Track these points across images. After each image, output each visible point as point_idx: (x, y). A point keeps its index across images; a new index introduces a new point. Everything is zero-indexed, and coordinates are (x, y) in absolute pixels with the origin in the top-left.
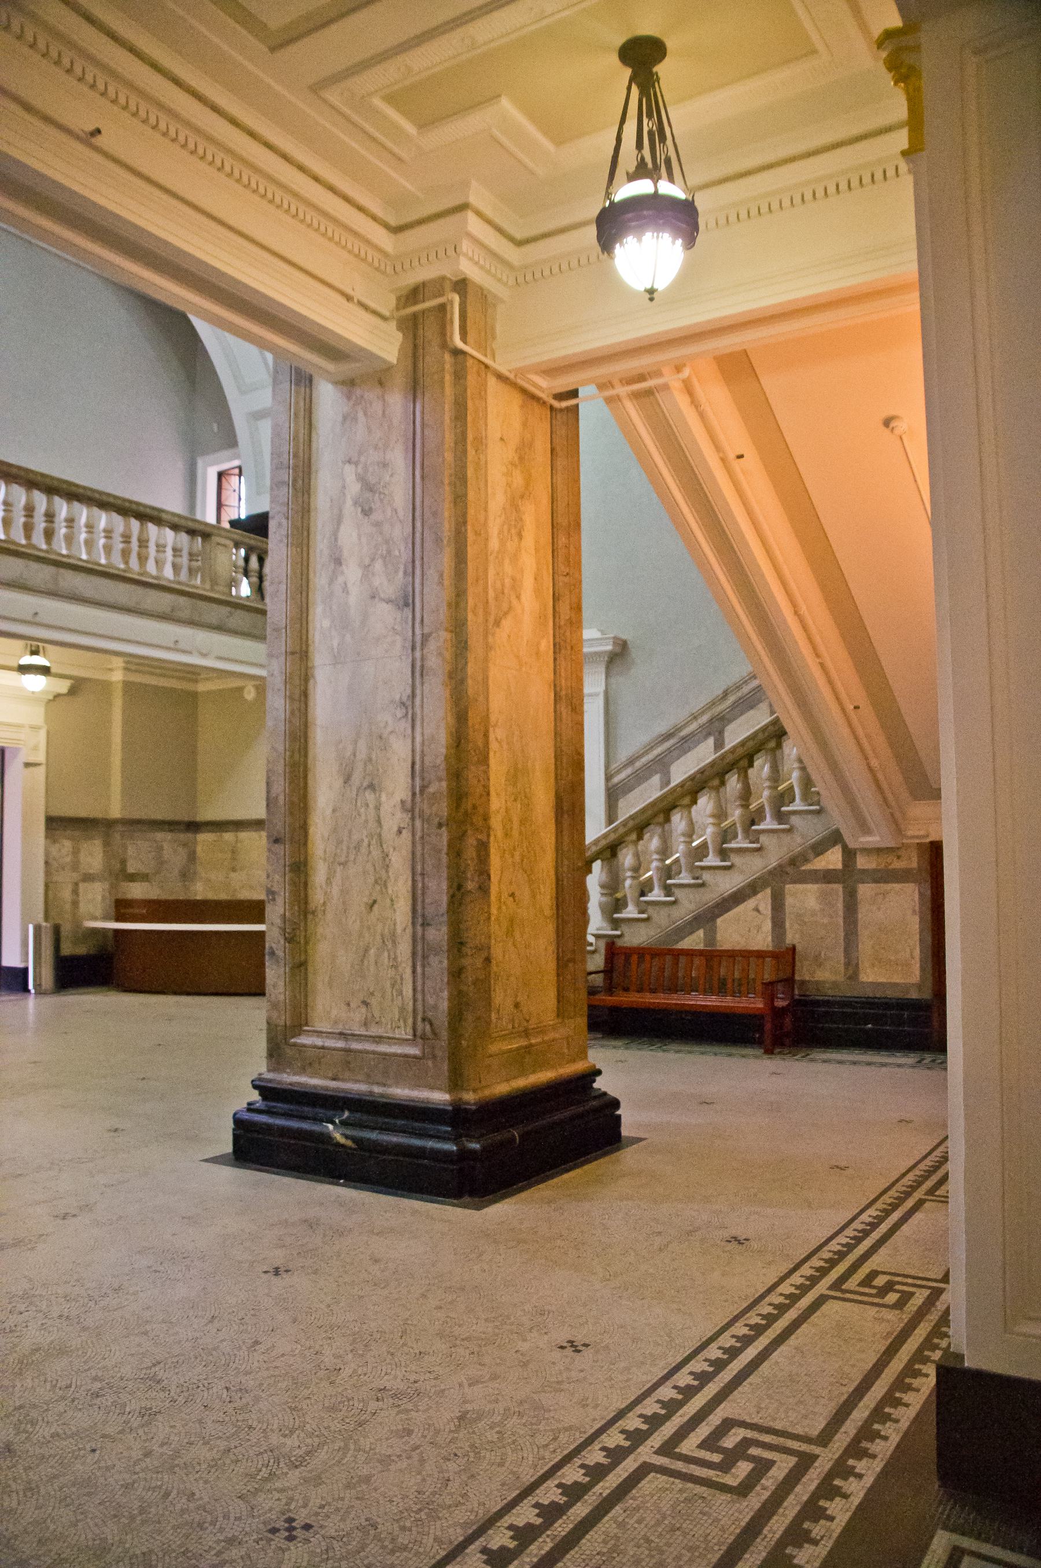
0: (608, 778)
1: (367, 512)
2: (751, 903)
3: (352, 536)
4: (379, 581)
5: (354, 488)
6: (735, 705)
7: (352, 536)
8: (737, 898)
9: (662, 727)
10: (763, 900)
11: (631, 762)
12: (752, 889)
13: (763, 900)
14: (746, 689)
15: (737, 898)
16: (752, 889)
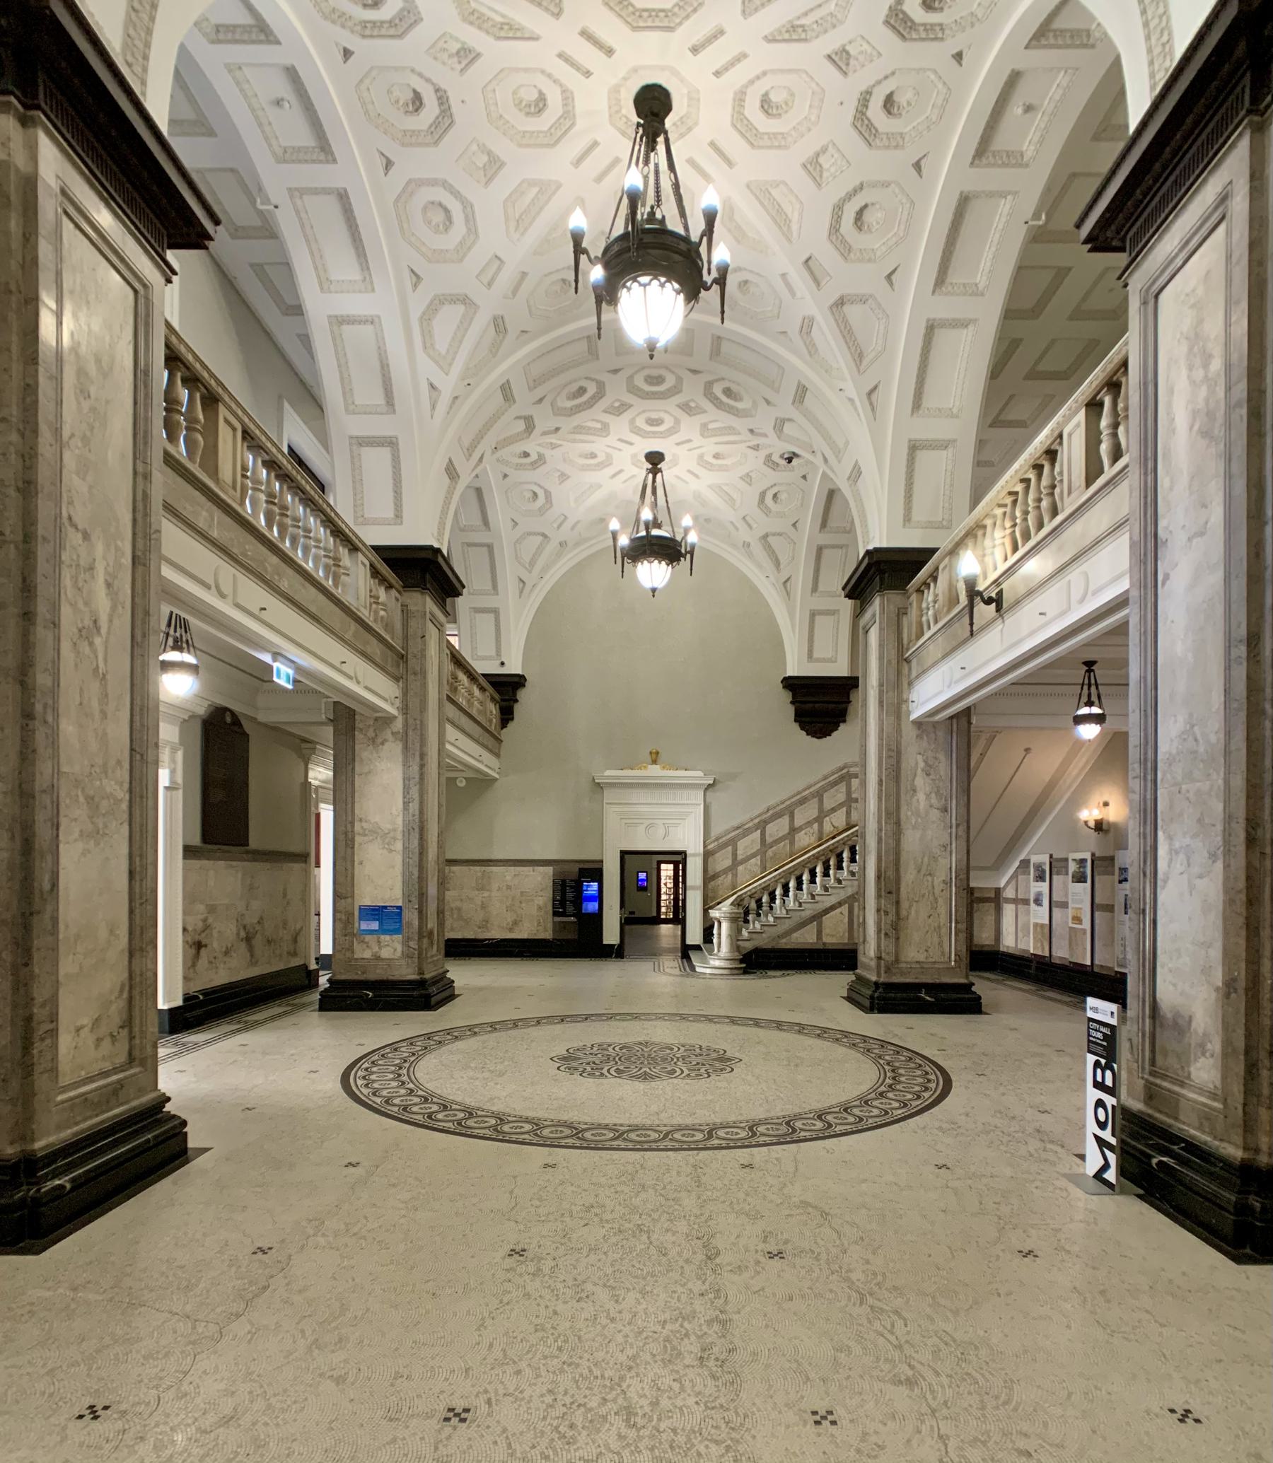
0: (705, 847)
1: (928, 775)
2: (838, 910)
3: (102, 603)
4: (934, 801)
5: (921, 765)
6: (772, 816)
7: (102, 603)
8: (832, 908)
9: (735, 823)
10: (845, 909)
11: (717, 839)
12: (840, 904)
13: (845, 909)
14: (778, 808)
15: (832, 908)
16: (840, 904)
